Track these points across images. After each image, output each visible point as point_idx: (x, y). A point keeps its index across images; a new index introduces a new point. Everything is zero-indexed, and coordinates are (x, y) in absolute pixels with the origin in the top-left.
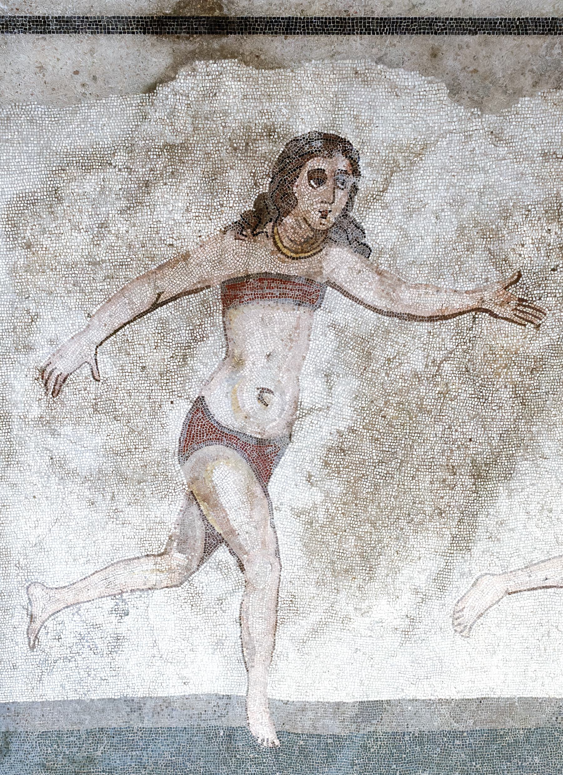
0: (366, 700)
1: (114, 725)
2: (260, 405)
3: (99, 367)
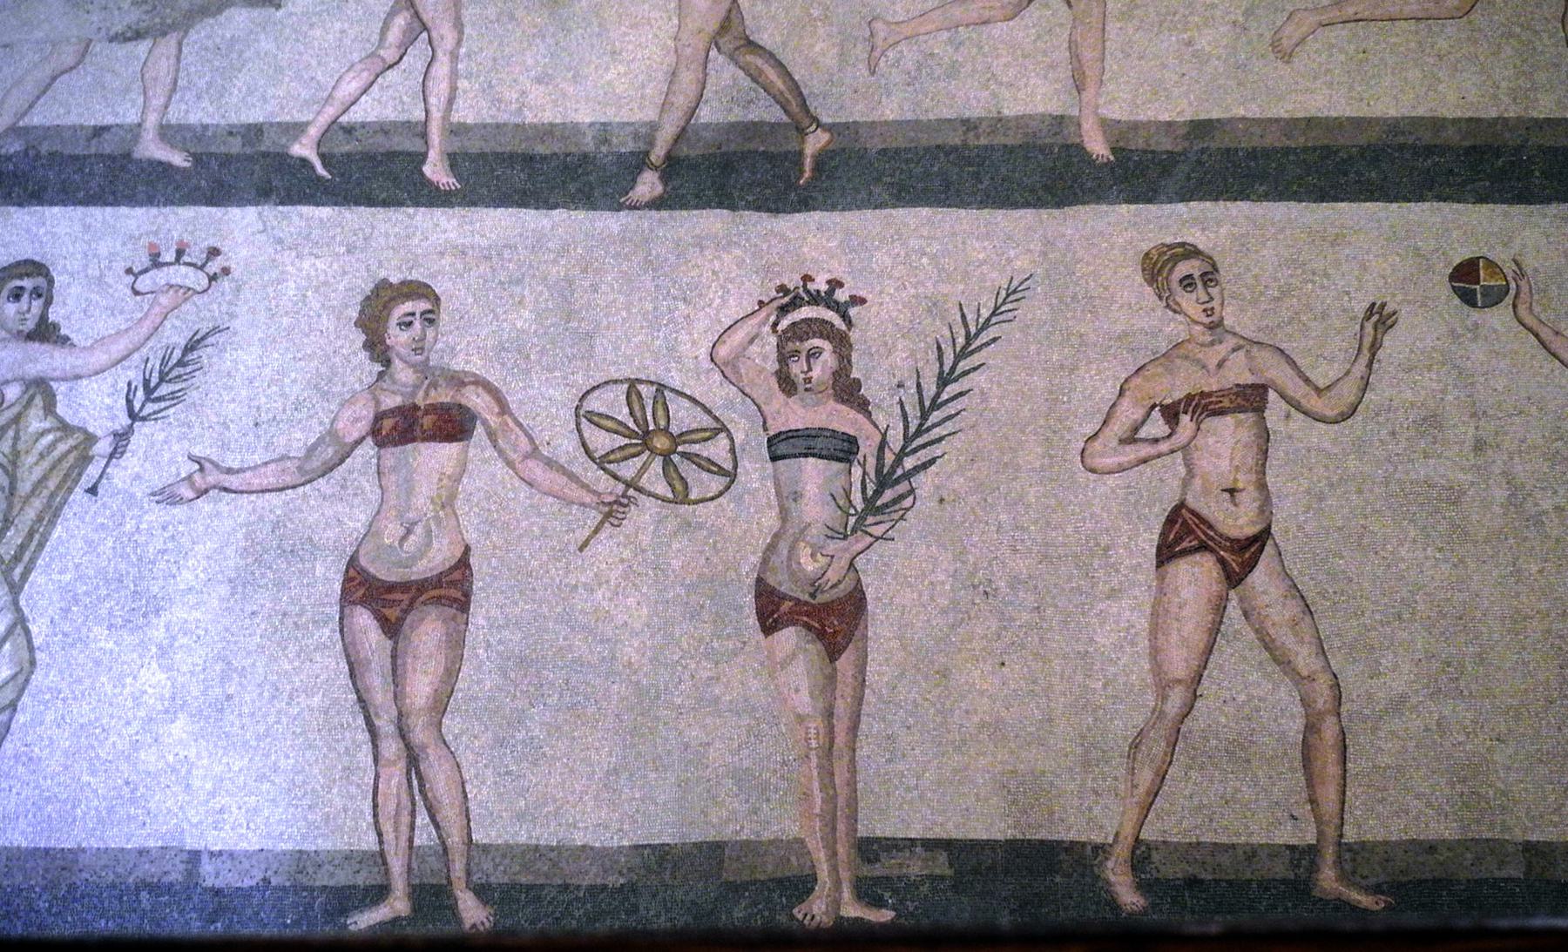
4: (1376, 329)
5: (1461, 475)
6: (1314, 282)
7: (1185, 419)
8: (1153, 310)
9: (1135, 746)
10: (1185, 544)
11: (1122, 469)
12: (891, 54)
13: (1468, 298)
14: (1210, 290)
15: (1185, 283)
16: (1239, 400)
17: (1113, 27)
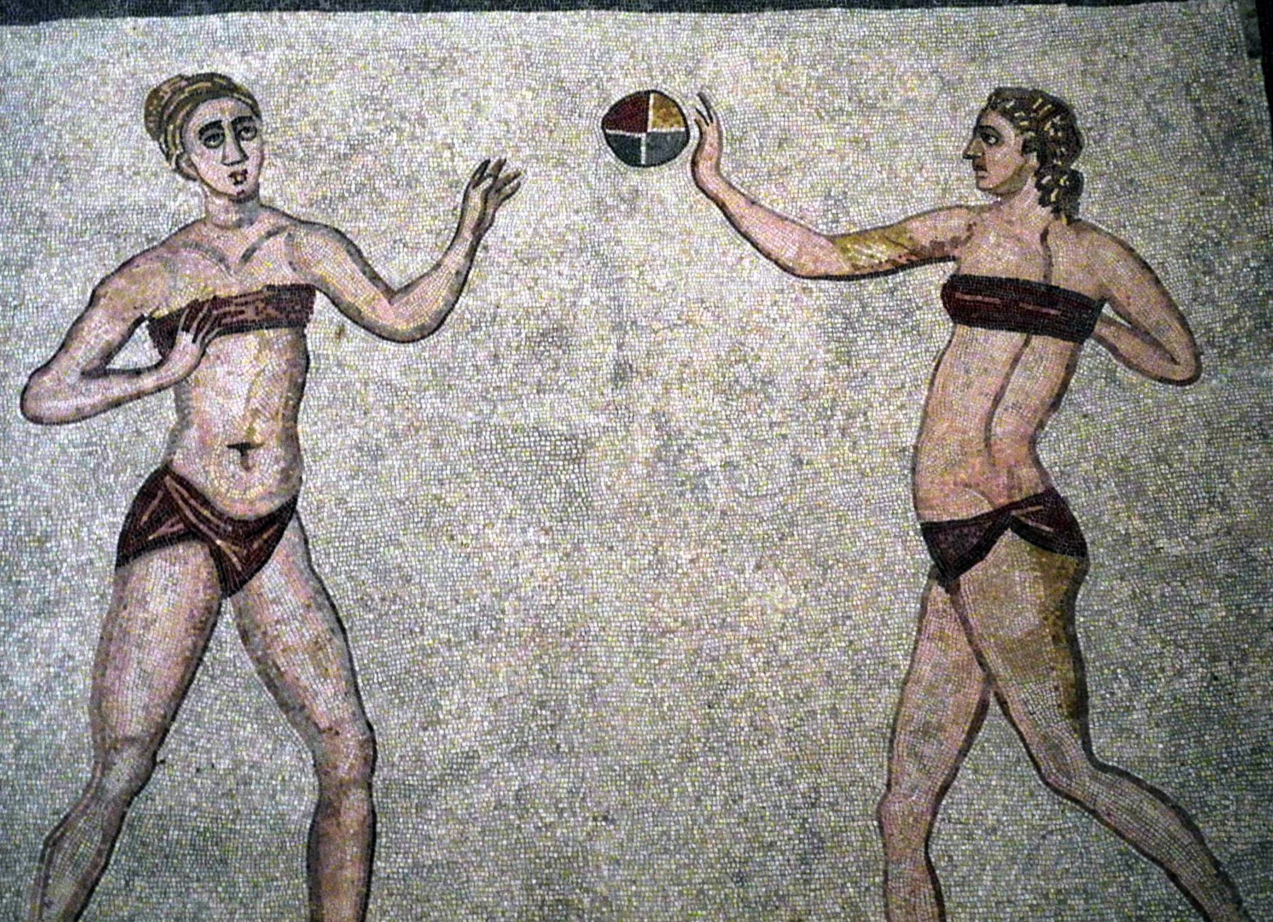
4: (485, 200)
5: (591, 420)
6: (400, 131)
7: (185, 339)
8: (156, 175)
9: (53, 842)
10: (163, 530)
11: (81, 416)
13: (627, 153)
14: (243, 144)
15: (210, 133)
16: (270, 310)
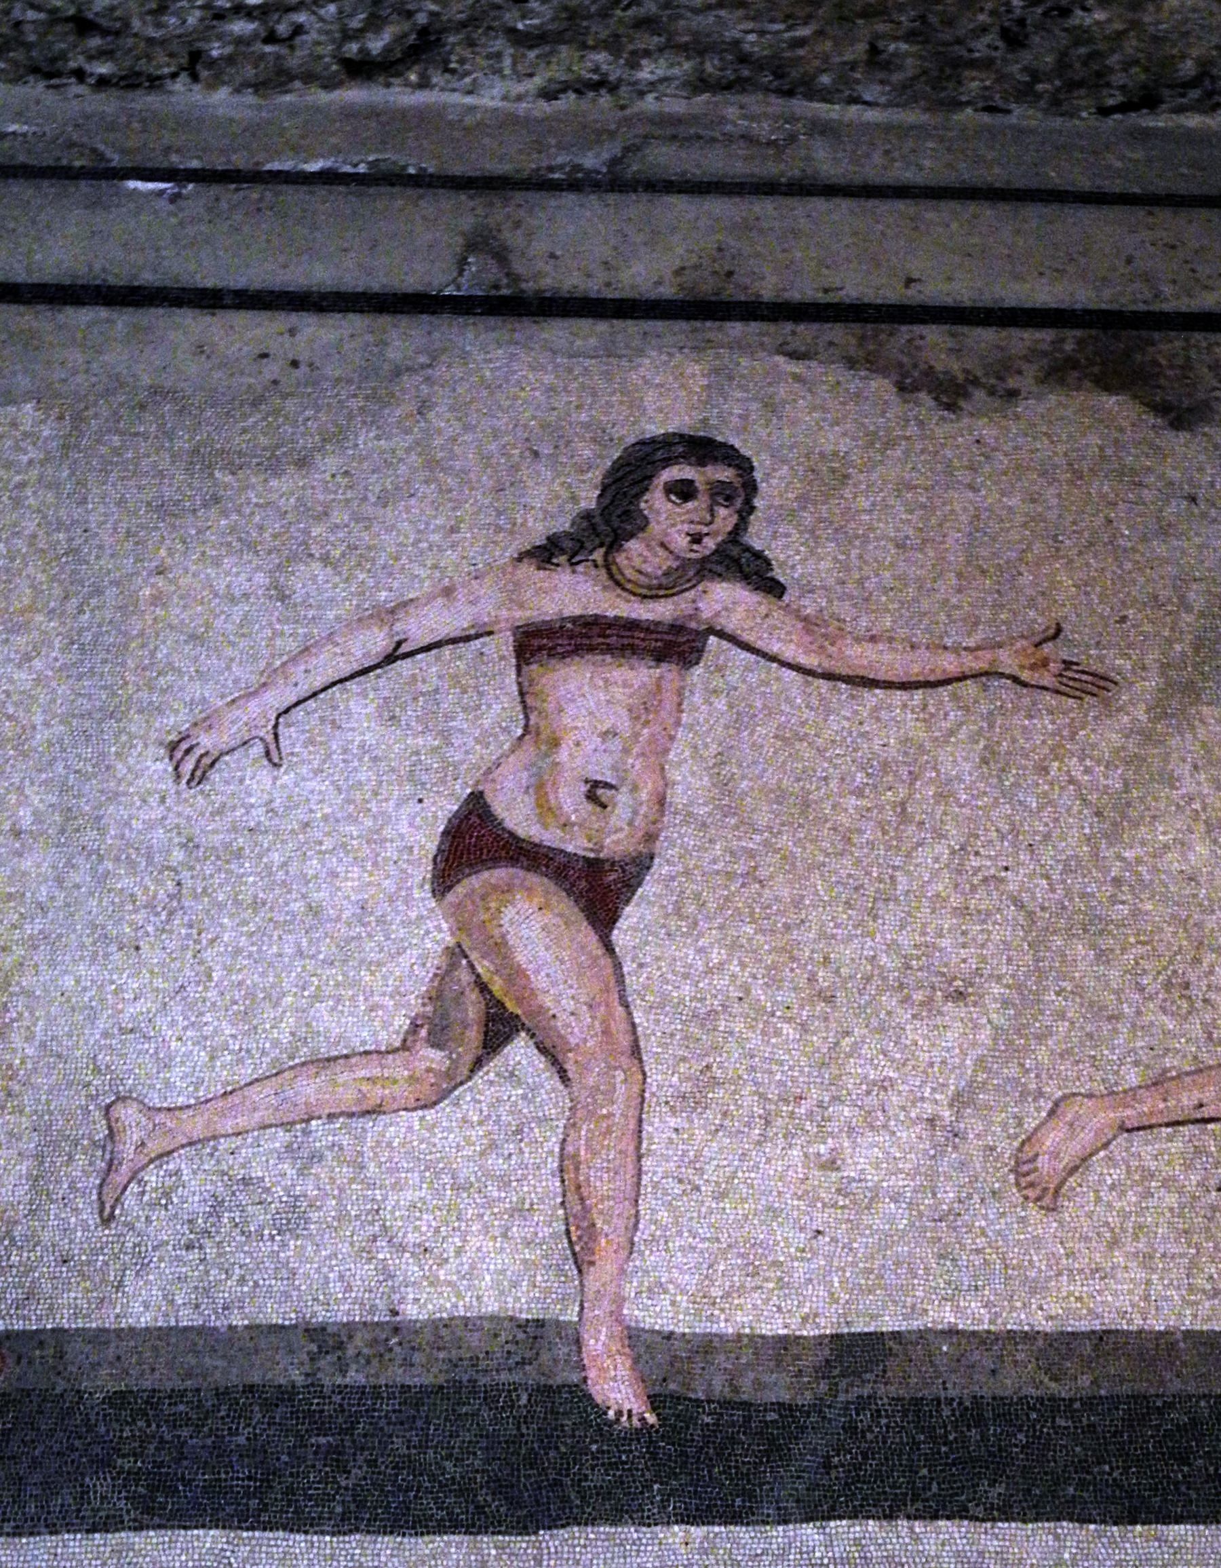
0: (846, 1330)
1: (282, 1381)
2: (590, 807)
3: (282, 745)
12: (152, 1177)
17: (659, 1127)
